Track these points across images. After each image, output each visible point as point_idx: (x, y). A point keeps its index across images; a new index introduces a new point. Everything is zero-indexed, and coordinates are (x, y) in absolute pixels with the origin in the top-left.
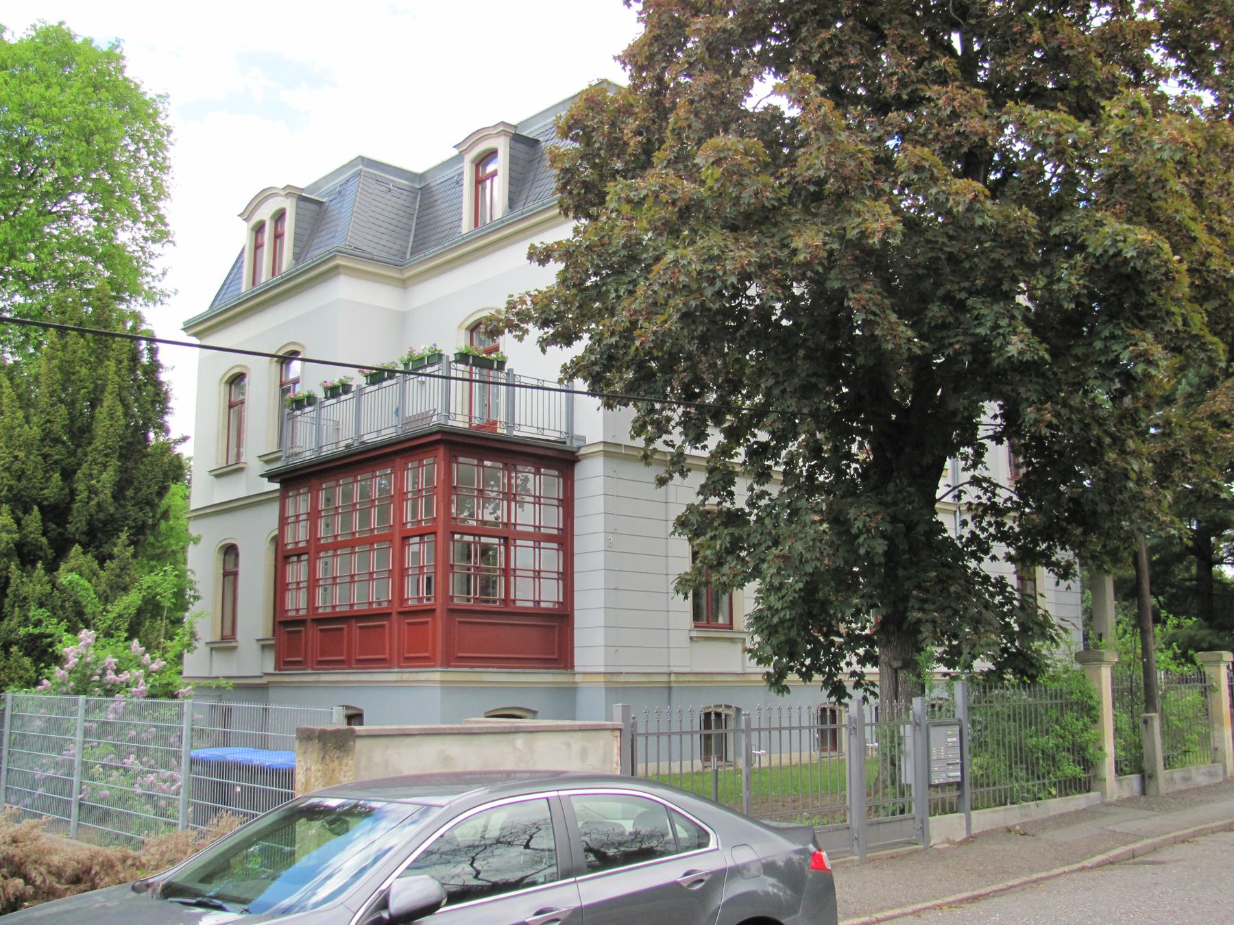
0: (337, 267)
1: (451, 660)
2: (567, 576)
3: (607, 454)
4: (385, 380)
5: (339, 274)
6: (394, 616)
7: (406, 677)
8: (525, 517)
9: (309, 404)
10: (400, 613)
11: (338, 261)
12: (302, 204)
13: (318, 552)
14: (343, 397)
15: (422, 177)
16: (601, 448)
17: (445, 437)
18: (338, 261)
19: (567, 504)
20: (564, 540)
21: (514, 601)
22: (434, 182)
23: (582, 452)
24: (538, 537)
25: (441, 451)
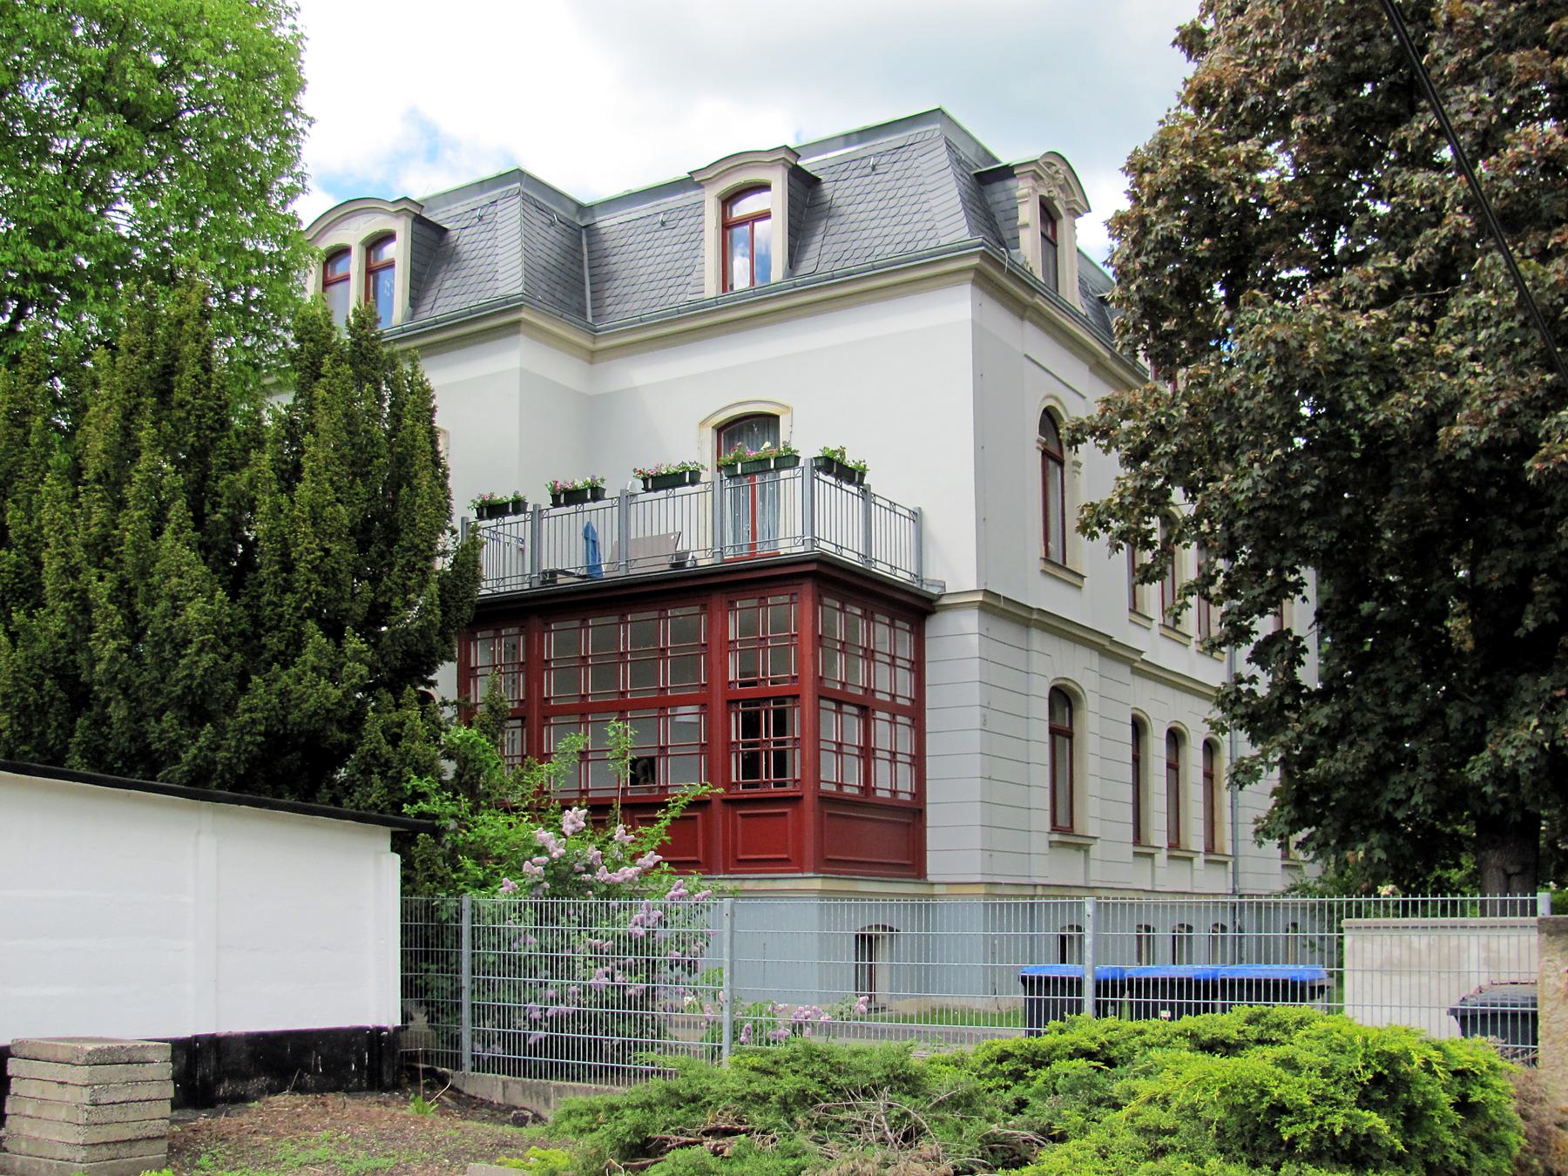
0: (517, 323)
1: (829, 864)
2: (918, 761)
3: (983, 607)
4: (685, 484)
5: (518, 332)
6: (717, 808)
7: (749, 885)
8: (883, 681)
9: (516, 512)
10: (726, 801)
11: (523, 315)
12: (418, 227)
13: (547, 718)
14: (587, 506)
15: (582, 209)
16: (980, 598)
17: (825, 570)
18: (523, 315)
19: (918, 667)
20: (916, 713)
21: (874, 789)
22: (607, 222)
23: (945, 601)
24: (894, 710)
25: (808, 588)
